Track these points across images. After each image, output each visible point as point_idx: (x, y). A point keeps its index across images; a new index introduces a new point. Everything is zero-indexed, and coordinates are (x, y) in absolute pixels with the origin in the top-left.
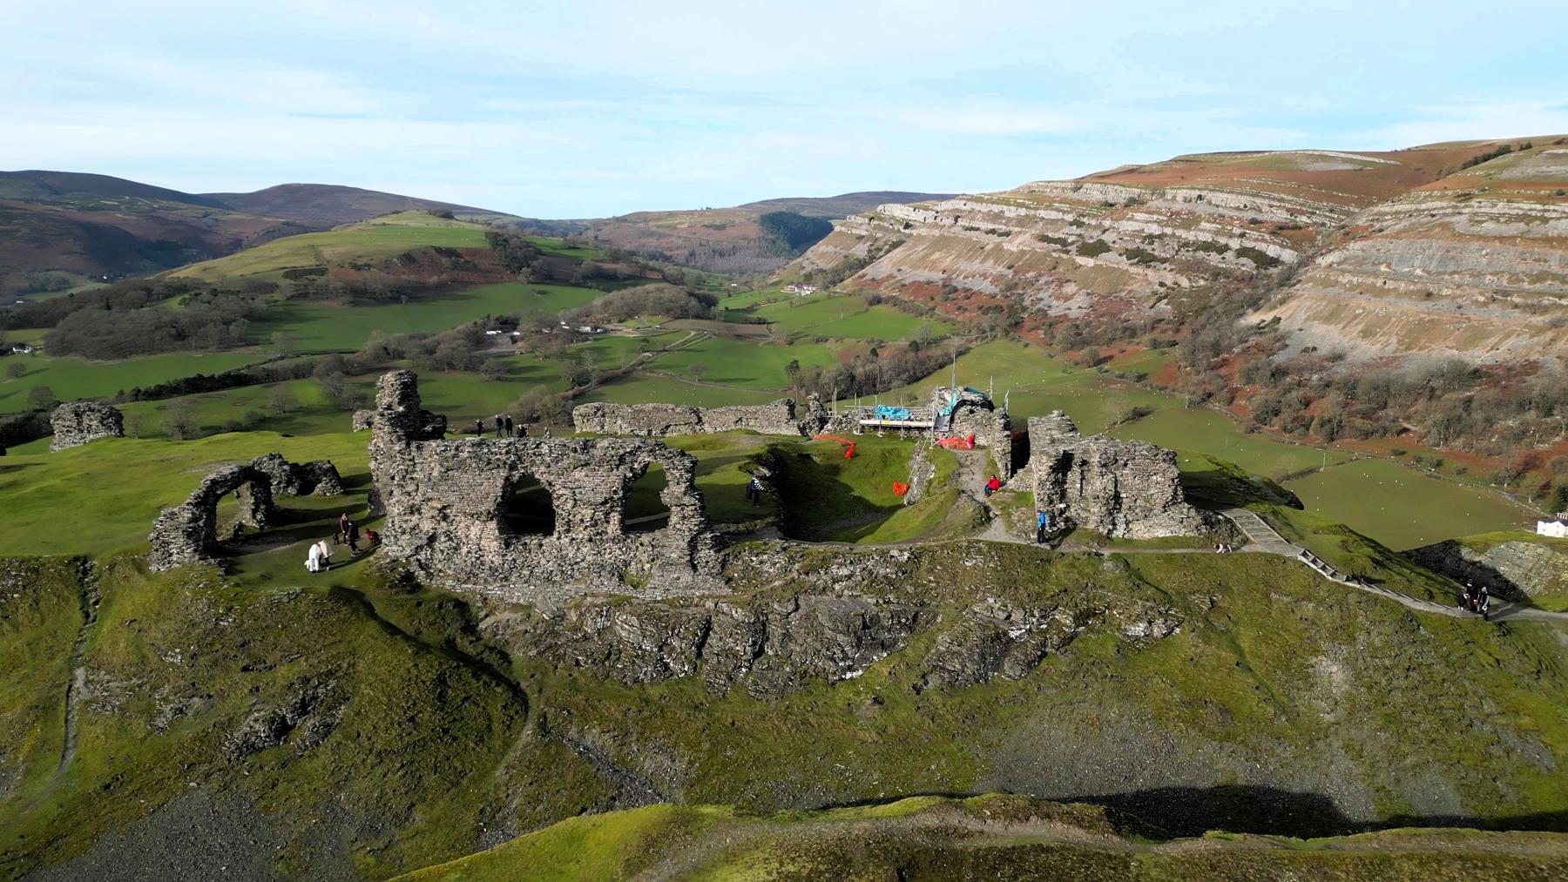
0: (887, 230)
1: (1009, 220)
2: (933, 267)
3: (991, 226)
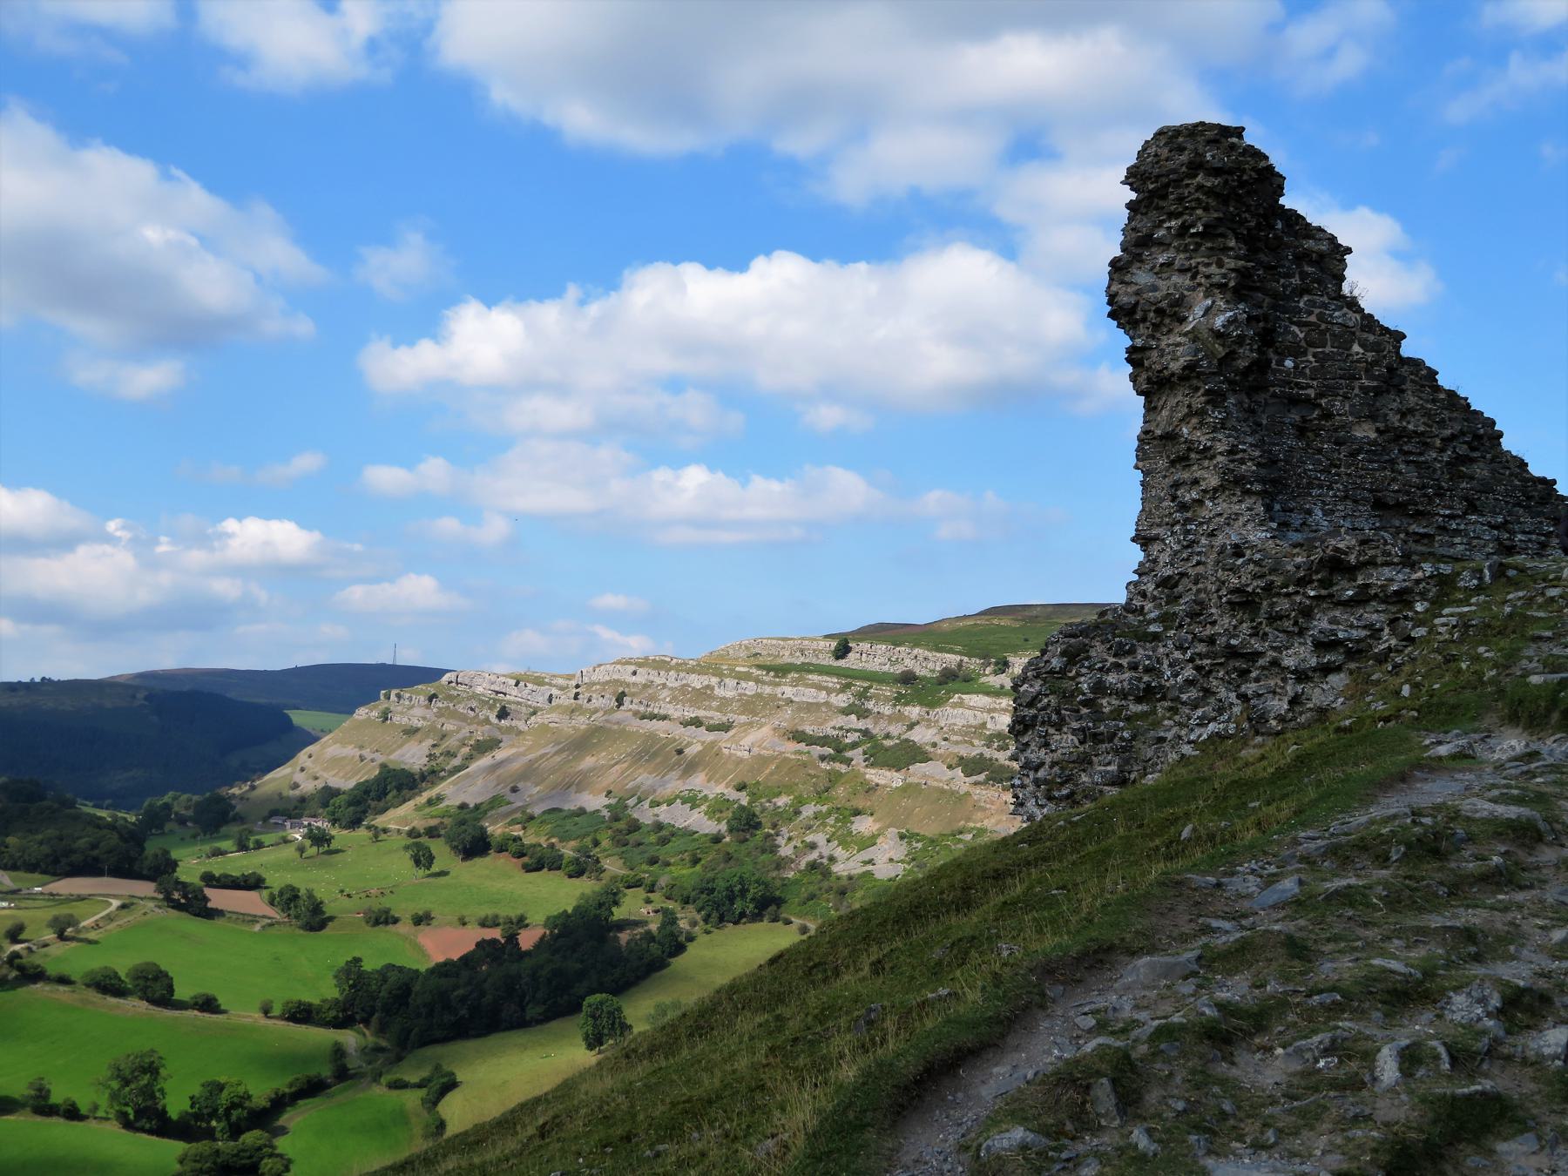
1: (725, 703)
3: (691, 713)
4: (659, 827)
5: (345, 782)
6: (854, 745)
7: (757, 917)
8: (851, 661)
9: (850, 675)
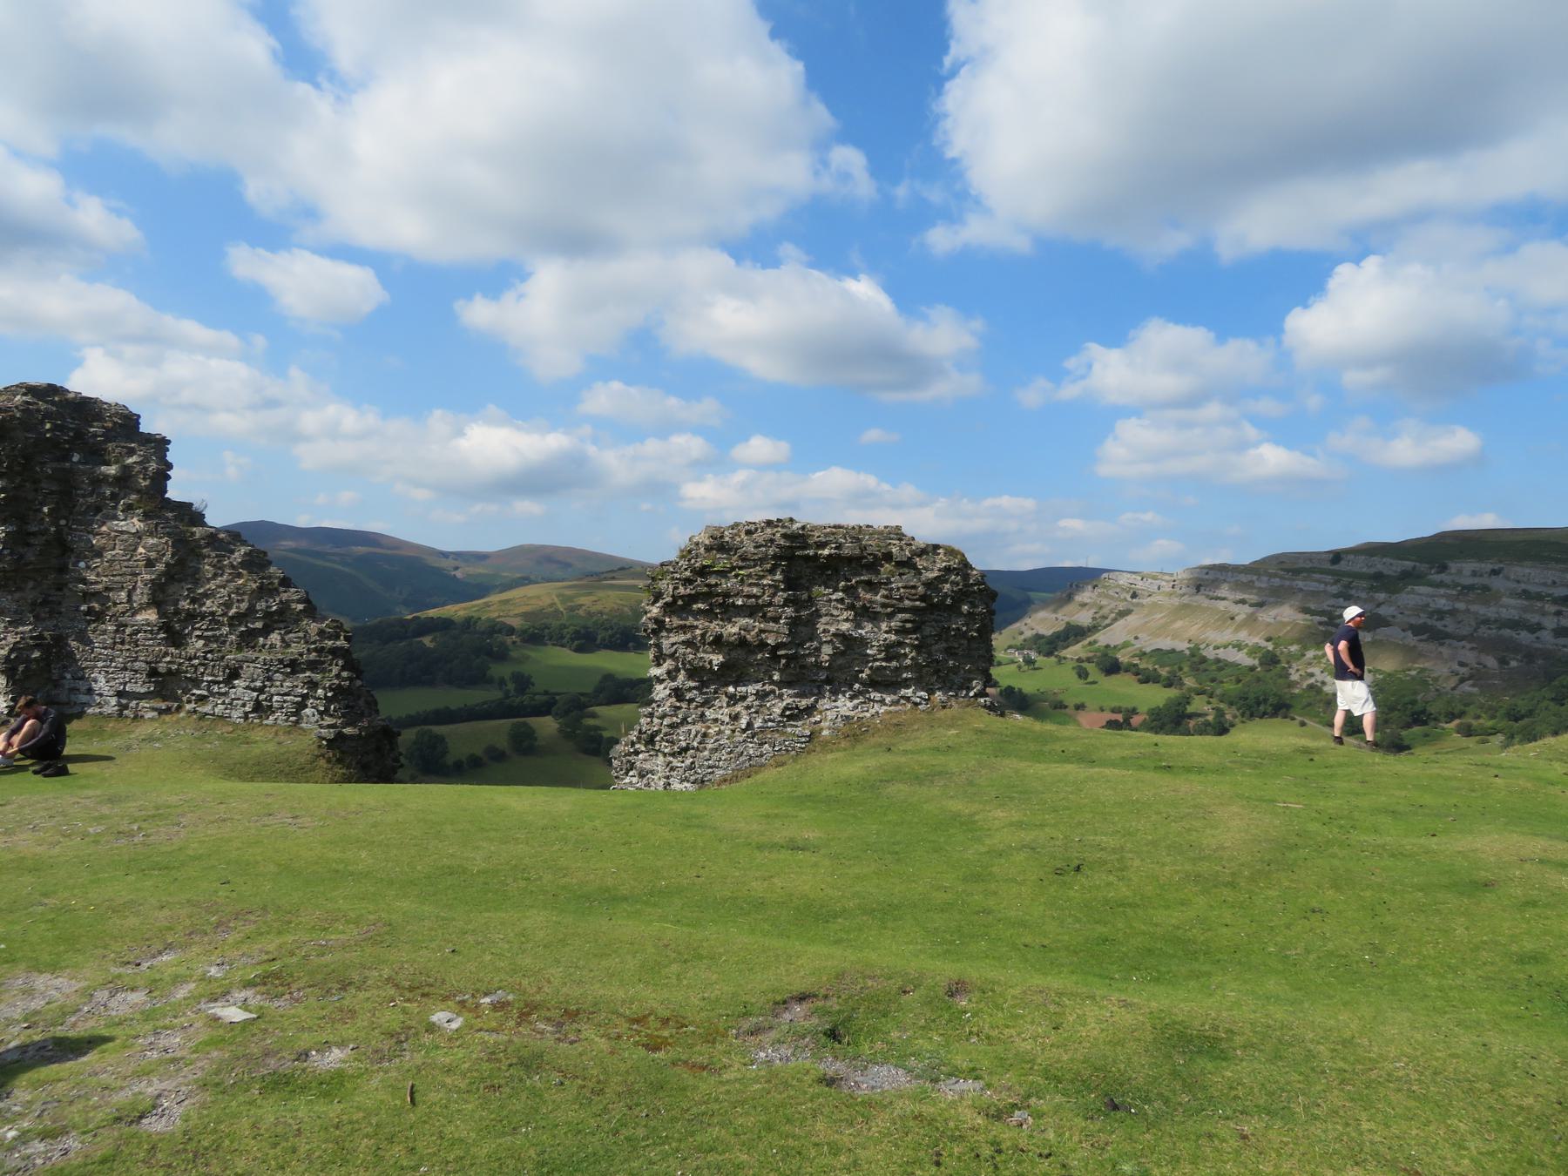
0: (1112, 598)
2: (1174, 637)
3: (1240, 596)
4: (1218, 661)
5: (1047, 631)
7: (1274, 715)
8: (1343, 566)
9: (1338, 576)
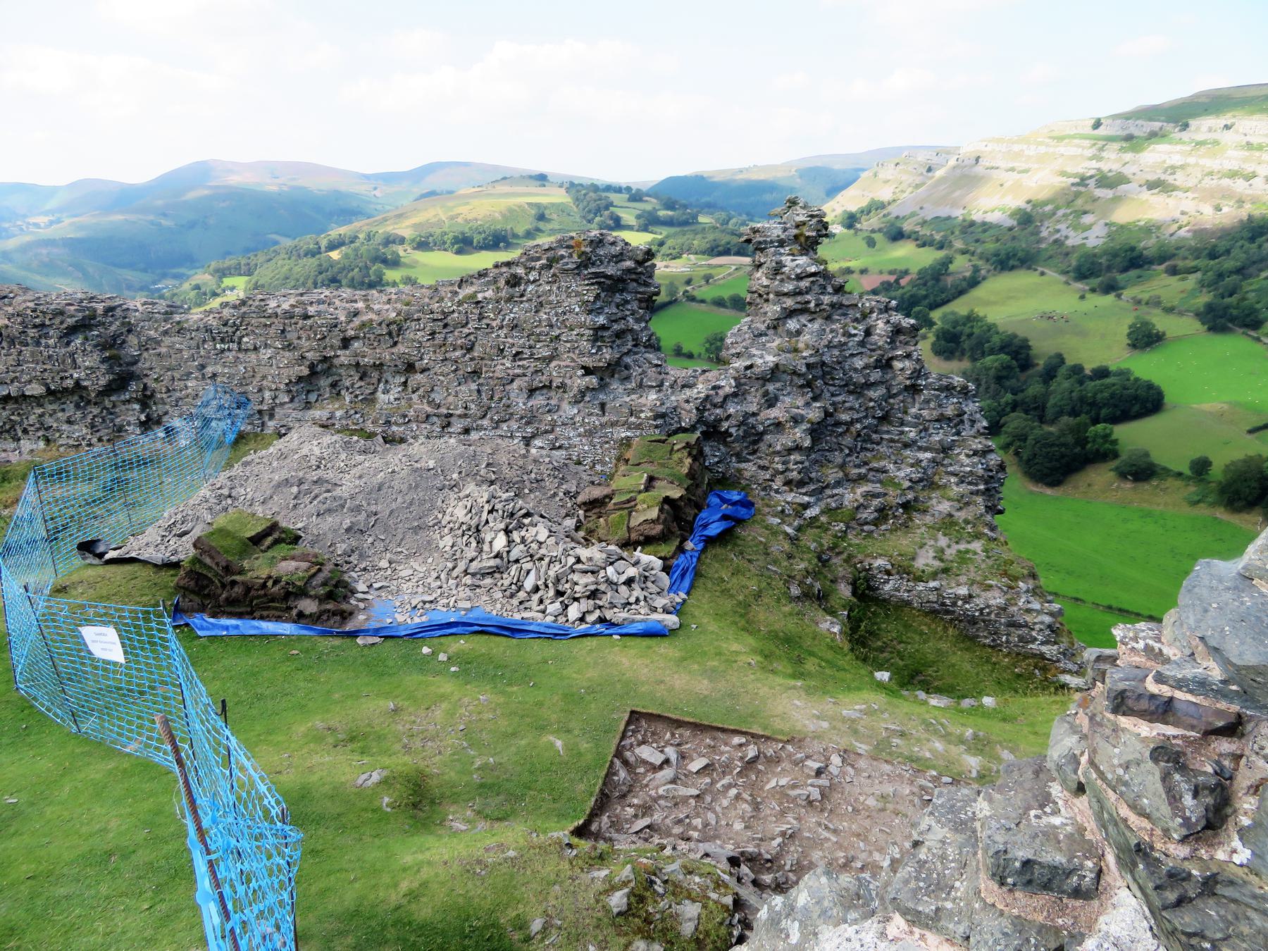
4: (984, 224)
6: (1091, 177)
